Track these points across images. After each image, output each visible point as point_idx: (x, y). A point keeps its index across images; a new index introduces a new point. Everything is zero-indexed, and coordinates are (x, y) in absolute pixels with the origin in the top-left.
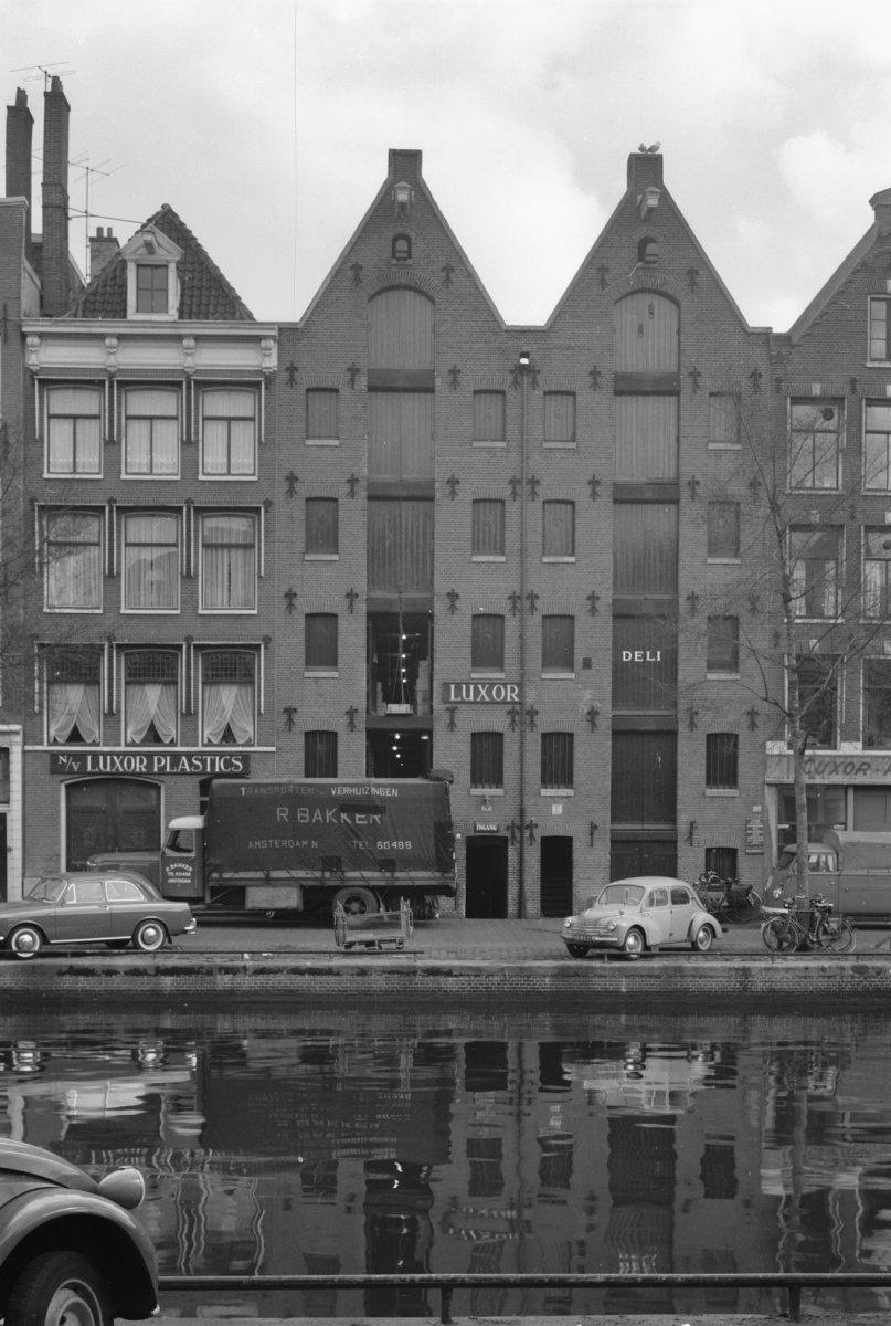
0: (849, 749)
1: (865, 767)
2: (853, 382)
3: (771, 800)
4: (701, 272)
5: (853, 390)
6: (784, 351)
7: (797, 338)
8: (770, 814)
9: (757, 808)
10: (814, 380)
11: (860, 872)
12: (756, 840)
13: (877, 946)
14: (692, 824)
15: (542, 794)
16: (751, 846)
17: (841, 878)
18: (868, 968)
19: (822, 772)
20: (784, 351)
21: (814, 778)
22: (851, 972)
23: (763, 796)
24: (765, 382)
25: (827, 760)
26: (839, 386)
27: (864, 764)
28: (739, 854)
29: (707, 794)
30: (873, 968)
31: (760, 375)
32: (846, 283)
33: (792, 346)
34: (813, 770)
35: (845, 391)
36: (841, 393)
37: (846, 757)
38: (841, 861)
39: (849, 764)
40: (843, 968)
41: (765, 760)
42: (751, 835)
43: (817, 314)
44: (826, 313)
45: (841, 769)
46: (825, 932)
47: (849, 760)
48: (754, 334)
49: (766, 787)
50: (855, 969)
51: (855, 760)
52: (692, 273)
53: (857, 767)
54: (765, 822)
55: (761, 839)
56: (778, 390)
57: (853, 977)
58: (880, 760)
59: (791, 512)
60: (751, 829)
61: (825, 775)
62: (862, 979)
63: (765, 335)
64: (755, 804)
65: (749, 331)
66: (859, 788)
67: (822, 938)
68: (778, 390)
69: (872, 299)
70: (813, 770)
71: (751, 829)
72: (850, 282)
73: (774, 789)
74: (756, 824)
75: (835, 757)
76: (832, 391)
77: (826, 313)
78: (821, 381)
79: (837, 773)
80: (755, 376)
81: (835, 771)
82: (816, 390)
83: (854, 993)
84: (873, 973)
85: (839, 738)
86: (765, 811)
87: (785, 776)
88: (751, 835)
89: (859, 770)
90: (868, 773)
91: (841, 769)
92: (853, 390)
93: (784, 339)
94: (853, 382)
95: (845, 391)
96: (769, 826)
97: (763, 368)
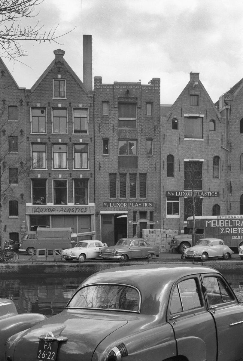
0: (71, 204)
1: (54, 210)
2: (49, 103)
3: (28, 219)
4: (5, 72)
5: (49, 105)
6: (29, 94)
7: (33, 90)
8: (28, 223)
9: (24, 221)
10: (38, 103)
11: (43, 239)
12: (23, 230)
13: (29, 260)
14: (5, 226)
15: (10, 218)
16: (22, 232)
17: (38, 241)
18: (9, 266)
19: (42, 211)
20: (29, 94)
21: (39, 213)
22: (5, 267)
23: (25, 218)
24: (24, 103)
25: (43, 208)
26: (45, 104)
27: (53, 209)
28: (19, 234)
29: (10, 218)
30: (11, 266)
31: (23, 101)
32: (46, 76)
33: (31, 93)
34: (39, 211)
35: (47, 106)
36: (66, 107)
37: (48, 207)
38: (38, 236)
39: (49, 209)
40: (2, 266)
41: (26, 208)
42: (22, 229)
43: (38, 84)
44: (41, 84)
45: (47, 210)
46: (6, 256)
47: (49, 208)
48: (20, 89)
49: (26, 215)
50: (6, 266)
51: (51, 208)
52: (3, 72)
53: (52, 209)
54: (26, 226)
55: (25, 230)
56: (28, 105)
57: (5, 269)
58: (58, 208)
59: (32, 140)
60: (22, 227)
61: (43, 212)
62: (8, 269)
63: (24, 90)
64: (23, 220)
65: (19, 89)
66: (53, 216)
67: (4, 257)
68: (28, 105)
69: (54, 80)
70: (39, 211)
71: (22, 227)
72: (48, 75)
73: (28, 216)
74: (23, 226)
75: (45, 207)
76: (43, 106)
77: (41, 84)
78: (40, 103)
79: (46, 211)
80: (21, 101)
81: (46, 211)
82: (39, 105)
83: (6, 273)
84: (11, 267)
85: (68, 202)
86: (26, 222)
87: (32, 212)
88: (22, 229)
89: (52, 210)
90: (55, 211)
91: (47, 210)
92: (49, 105)
93: (29, 91)
94: (49, 103)
95: (47, 106)
96: (27, 226)
97: (23, 99)
